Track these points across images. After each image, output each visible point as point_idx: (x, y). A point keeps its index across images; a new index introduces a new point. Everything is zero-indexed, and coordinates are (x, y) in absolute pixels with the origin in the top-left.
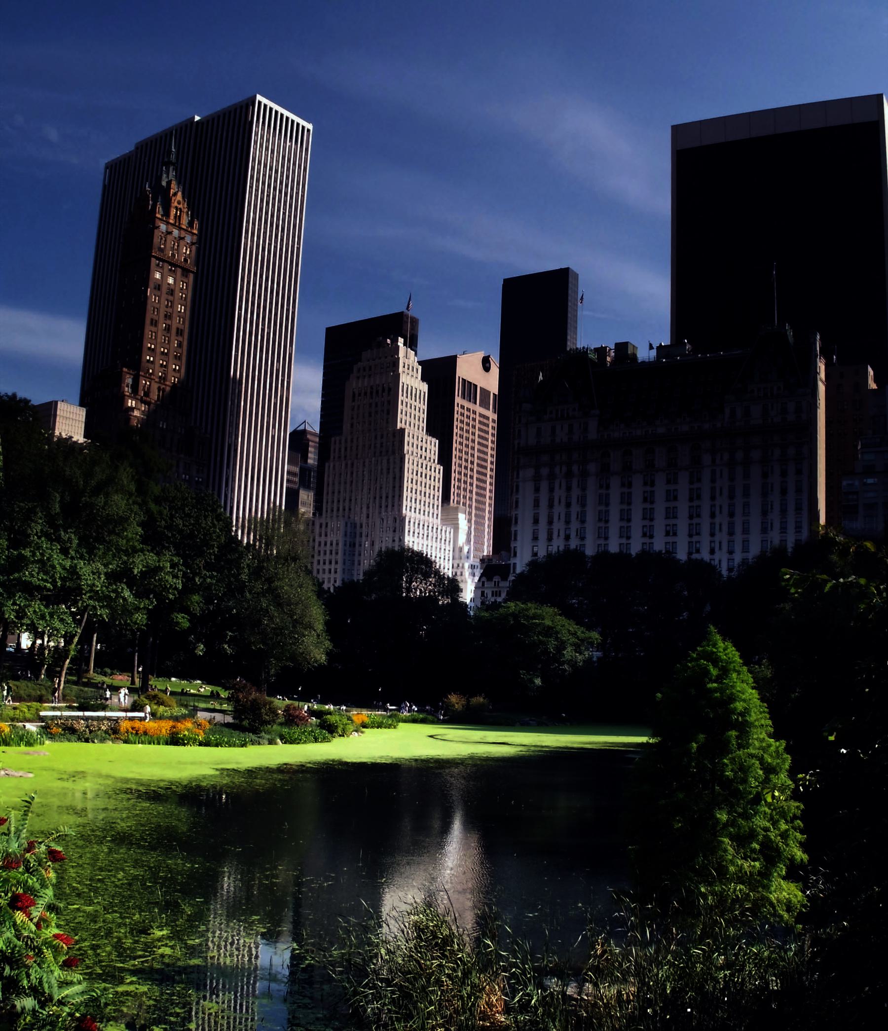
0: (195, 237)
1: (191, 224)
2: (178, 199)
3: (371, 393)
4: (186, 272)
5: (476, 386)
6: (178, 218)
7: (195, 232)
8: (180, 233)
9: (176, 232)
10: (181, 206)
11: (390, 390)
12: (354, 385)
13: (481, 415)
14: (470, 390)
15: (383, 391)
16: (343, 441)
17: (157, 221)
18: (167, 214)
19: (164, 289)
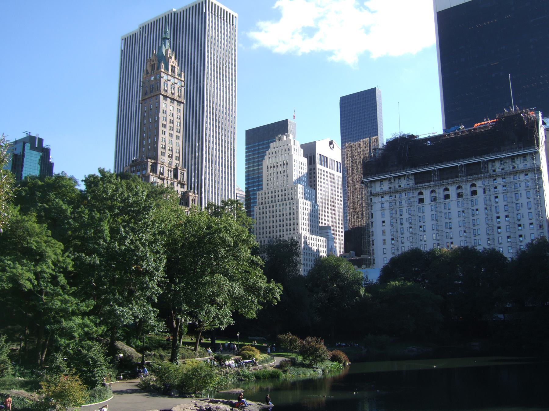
0: (183, 83)
1: (180, 75)
2: (172, 61)
3: (277, 166)
4: (179, 103)
5: (327, 158)
6: (173, 71)
7: (183, 79)
8: (175, 81)
9: (172, 80)
10: (174, 65)
11: (287, 164)
12: (267, 161)
13: (331, 174)
14: (325, 161)
15: (284, 164)
16: (263, 193)
17: (162, 73)
18: (167, 68)
19: (168, 113)
